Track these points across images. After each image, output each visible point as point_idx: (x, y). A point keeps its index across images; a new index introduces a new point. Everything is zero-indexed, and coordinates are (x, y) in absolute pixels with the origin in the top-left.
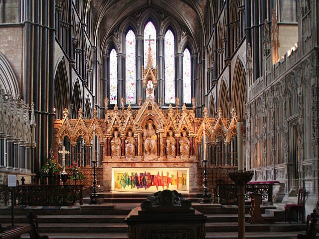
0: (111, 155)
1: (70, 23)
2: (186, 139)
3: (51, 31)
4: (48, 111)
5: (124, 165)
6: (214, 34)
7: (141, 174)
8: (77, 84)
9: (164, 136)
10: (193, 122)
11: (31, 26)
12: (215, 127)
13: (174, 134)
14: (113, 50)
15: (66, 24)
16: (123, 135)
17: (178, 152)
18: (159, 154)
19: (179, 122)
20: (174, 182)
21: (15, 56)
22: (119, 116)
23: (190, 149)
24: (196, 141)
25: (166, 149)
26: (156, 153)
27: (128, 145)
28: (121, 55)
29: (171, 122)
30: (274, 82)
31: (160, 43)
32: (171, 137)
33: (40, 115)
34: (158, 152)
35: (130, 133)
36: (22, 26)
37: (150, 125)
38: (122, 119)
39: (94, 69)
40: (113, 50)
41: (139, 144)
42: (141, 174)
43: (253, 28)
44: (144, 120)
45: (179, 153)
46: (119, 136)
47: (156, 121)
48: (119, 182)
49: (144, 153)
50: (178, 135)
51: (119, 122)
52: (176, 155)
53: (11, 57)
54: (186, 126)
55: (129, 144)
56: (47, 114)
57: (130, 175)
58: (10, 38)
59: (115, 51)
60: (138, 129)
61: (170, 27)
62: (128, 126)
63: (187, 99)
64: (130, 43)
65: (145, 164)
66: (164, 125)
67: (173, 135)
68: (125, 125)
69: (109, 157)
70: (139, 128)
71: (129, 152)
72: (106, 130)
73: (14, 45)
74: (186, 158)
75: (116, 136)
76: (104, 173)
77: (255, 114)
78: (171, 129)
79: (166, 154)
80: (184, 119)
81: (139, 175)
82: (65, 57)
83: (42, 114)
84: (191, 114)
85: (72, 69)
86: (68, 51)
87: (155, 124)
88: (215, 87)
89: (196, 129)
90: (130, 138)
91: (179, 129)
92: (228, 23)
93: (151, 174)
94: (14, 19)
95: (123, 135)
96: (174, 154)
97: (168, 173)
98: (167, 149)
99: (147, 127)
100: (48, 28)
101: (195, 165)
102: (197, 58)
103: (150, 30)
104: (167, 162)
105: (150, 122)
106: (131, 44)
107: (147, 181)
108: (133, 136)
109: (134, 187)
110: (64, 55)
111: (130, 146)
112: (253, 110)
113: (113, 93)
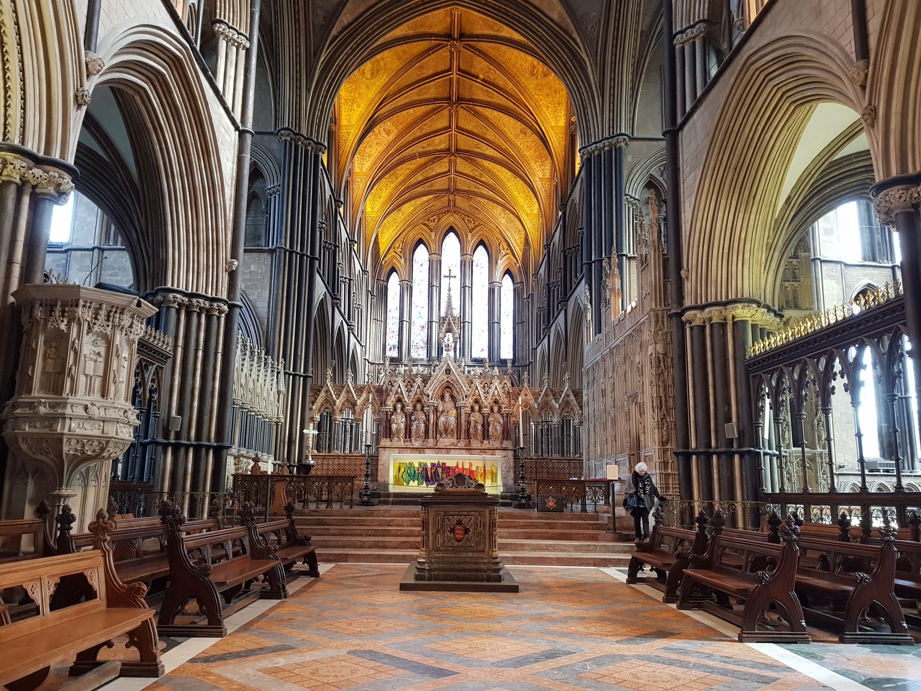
1: (335, 243)
2: (498, 416)
3: (312, 260)
4: (302, 371)
5: (409, 451)
6: (546, 258)
8: (341, 330)
10: (508, 392)
11: (285, 253)
13: (480, 408)
15: (330, 244)
16: (409, 408)
17: (486, 435)
18: (459, 438)
21: (259, 293)
23: (503, 431)
25: (468, 430)
26: (455, 435)
30: (613, 343)
31: (466, 265)
32: (477, 414)
33: (291, 377)
35: (419, 406)
36: (272, 251)
37: (447, 396)
39: (364, 304)
40: (394, 273)
42: (433, 465)
43: (594, 262)
45: (488, 436)
46: (403, 409)
49: (438, 436)
50: (486, 411)
53: (254, 294)
54: (498, 398)
55: (416, 422)
56: (301, 376)
57: (416, 465)
58: (253, 268)
60: (430, 401)
61: (482, 243)
62: (416, 396)
63: (507, 352)
64: (419, 264)
65: (436, 449)
66: (466, 397)
67: (480, 411)
68: (412, 394)
71: (417, 433)
73: (259, 277)
74: (497, 444)
75: (399, 410)
76: (380, 463)
77: (593, 385)
78: (476, 401)
79: (468, 436)
80: (496, 389)
82: (327, 293)
83: (294, 376)
84: (505, 381)
85: (336, 309)
86: (331, 283)
88: (547, 337)
89: (513, 402)
91: (488, 402)
92: (564, 248)
93: (448, 465)
94: (259, 239)
95: (409, 408)
96: (480, 437)
97: (471, 464)
99: (442, 398)
100: (307, 256)
101: (511, 453)
102: (523, 289)
103: (451, 243)
104: (469, 449)
107: (440, 474)
108: (422, 410)
109: (422, 483)
110: (326, 290)
111: (419, 426)
112: (591, 378)
113: (392, 340)
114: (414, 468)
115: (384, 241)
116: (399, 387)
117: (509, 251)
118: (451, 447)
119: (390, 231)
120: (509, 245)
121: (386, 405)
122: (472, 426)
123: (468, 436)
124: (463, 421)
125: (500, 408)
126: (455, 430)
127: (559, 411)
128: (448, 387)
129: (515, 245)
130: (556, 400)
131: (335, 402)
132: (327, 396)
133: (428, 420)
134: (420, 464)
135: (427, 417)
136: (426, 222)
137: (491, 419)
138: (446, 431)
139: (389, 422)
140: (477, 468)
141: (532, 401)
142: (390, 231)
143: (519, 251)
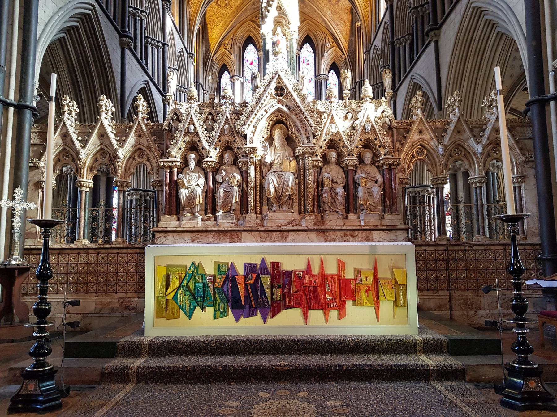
0: (178, 213)
5: (211, 236)
7: (250, 268)
9: (316, 163)
12: (446, 141)
14: (226, 72)
18: (302, 211)
20: (363, 294)
22: (201, 113)
24: (399, 175)
25: (320, 196)
34: (299, 204)
40: (226, 72)
42: (250, 268)
47: (296, 127)
48: (170, 297)
49: (265, 208)
50: (351, 160)
52: (348, 211)
57: (210, 270)
59: (228, 74)
62: (223, 139)
64: (249, 62)
74: (373, 220)
75: (192, 164)
79: (320, 208)
81: (241, 271)
86: (119, 17)
87: (293, 132)
90: (228, 169)
93: (286, 267)
96: (341, 209)
97: (341, 265)
98: (325, 195)
106: (251, 64)
107: (268, 291)
108: (235, 163)
109: (224, 314)
114: (204, 276)
115: (213, 37)
116: (192, 122)
117: (334, 44)
118: (290, 227)
119: (220, 27)
120: (335, 39)
121: (168, 155)
122: (326, 188)
123: (320, 208)
124: (309, 180)
126: (295, 197)
127: (482, 158)
129: (341, 37)
130: (477, 138)
131: (78, 153)
132: (64, 143)
134: (218, 266)
136: (254, 19)
137: (360, 175)
139: (175, 186)
140: (358, 272)
141: (433, 143)
142: (220, 27)
143: (343, 41)
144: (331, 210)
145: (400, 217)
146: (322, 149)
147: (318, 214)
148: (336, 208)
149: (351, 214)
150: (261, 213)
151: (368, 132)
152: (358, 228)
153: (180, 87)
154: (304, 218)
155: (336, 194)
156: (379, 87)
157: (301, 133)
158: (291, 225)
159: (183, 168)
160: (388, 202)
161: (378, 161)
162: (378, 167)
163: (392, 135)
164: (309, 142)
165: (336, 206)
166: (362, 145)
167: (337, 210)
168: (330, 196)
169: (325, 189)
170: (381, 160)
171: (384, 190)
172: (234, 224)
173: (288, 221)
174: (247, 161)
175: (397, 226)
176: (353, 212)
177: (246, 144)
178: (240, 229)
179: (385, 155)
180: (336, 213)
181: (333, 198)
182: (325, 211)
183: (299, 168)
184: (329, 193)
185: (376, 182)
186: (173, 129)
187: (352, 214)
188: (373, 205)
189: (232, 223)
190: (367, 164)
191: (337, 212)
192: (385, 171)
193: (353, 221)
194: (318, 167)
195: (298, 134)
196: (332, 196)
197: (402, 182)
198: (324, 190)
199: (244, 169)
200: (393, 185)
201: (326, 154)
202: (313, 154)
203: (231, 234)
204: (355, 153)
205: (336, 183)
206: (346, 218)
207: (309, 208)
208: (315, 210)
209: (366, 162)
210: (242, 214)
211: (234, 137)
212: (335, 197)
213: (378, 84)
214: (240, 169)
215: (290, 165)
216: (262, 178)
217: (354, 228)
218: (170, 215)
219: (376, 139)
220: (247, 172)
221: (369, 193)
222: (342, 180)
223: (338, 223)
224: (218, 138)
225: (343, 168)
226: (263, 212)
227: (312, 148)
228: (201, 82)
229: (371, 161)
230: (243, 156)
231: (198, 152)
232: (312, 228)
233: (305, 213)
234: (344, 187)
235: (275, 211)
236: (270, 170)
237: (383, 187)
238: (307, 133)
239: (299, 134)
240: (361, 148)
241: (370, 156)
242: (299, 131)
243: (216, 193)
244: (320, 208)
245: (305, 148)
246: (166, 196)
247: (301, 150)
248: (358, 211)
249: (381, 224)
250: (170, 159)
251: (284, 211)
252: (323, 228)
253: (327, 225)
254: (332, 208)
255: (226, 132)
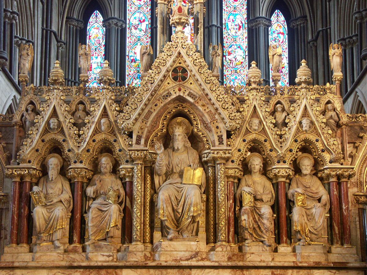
0: (29, 241)
9: (231, 172)
13: (266, 164)
19: (285, 124)
23: (330, 219)
24: (353, 190)
25: (237, 219)
26: (202, 234)
27: (94, 205)
28: (115, 21)
29: (256, 121)
34: (207, 230)
35: (105, 162)
37: (179, 133)
38: (80, 113)
41: (138, 200)
44: (159, 116)
46: (63, 172)
47: (203, 122)
49: (157, 235)
51: (67, 122)
52: (278, 241)
55: (99, 200)
59: (100, 16)
60: (135, 147)
62: (98, 137)
67: (265, 172)
69: (25, 247)
70: (138, 143)
72: (18, 150)
75: (53, 173)
96: (269, 237)
98: (244, 217)
102: (305, 29)
104: (242, 268)
105: (179, 124)
116: (54, 114)
118: (193, 263)
125: (317, 164)
126: (202, 220)
128: (180, 114)
133: (130, 195)
135: (128, 186)
138: (178, 222)
144: (254, 239)
145: (354, 250)
146: (240, 153)
147: (235, 244)
148: (260, 236)
149: (282, 245)
150: (152, 242)
151: (306, 131)
152: (292, 264)
153: (21, 39)
154: (213, 249)
155: (260, 216)
156: (354, 42)
157: (210, 131)
158: (194, 259)
159: (40, 178)
160: (336, 228)
161: (321, 171)
162: (321, 179)
163: (342, 135)
164: (221, 143)
165: (260, 233)
166: (298, 148)
167: (262, 239)
168: (251, 218)
169: (244, 208)
170: (326, 169)
171: (330, 211)
172: (111, 258)
173: (190, 253)
174: (132, 169)
175: (348, 263)
176: (286, 243)
177: (131, 145)
178: (121, 264)
179: (331, 162)
180: (261, 243)
181: (256, 222)
182: (246, 239)
183: (207, 178)
184: (250, 215)
185: (319, 200)
186: (27, 123)
187: (285, 245)
188: (315, 232)
189: (109, 256)
190: (306, 175)
191: (262, 242)
192: (331, 184)
193: (285, 255)
194: (234, 177)
195: (206, 132)
196: (254, 218)
197: (358, 202)
198: (242, 210)
199: (127, 180)
200: (344, 205)
201: (247, 160)
202: (227, 159)
203: (107, 272)
204: (289, 158)
205: (261, 200)
206: (276, 250)
207: (222, 236)
208: (231, 239)
209: (304, 172)
210: (123, 242)
211: (115, 135)
212: (259, 220)
213: (351, 38)
214: (121, 179)
215: (194, 174)
216: (152, 192)
217: (286, 264)
218: (18, 244)
219: (317, 141)
220: (131, 183)
221: (308, 215)
222: (270, 196)
223: (263, 258)
224: (91, 137)
225: (270, 179)
226: (154, 241)
227: (225, 151)
228: (54, 28)
229: (312, 171)
230: (127, 162)
231: (61, 155)
232: (225, 264)
233: (215, 242)
234: (272, 207)
235: (171, 240)
236: (165, 181)
237: (328, 207)
238: (218, 131)
239: (208, 132)
240: (297, 152)
241: (308, 164)
242: (207, 127)
243: (86, 213)
244: (238, 235)
245: (216, 153)
246: (13, 217)
247: (209, 153)
248: (292, 240)
249: (327, 260)
250: (21, 165)
251: (184, 239)
252: (241, 264)
253: (248, 260)
254: (254, 235)
255: (103, 128)
